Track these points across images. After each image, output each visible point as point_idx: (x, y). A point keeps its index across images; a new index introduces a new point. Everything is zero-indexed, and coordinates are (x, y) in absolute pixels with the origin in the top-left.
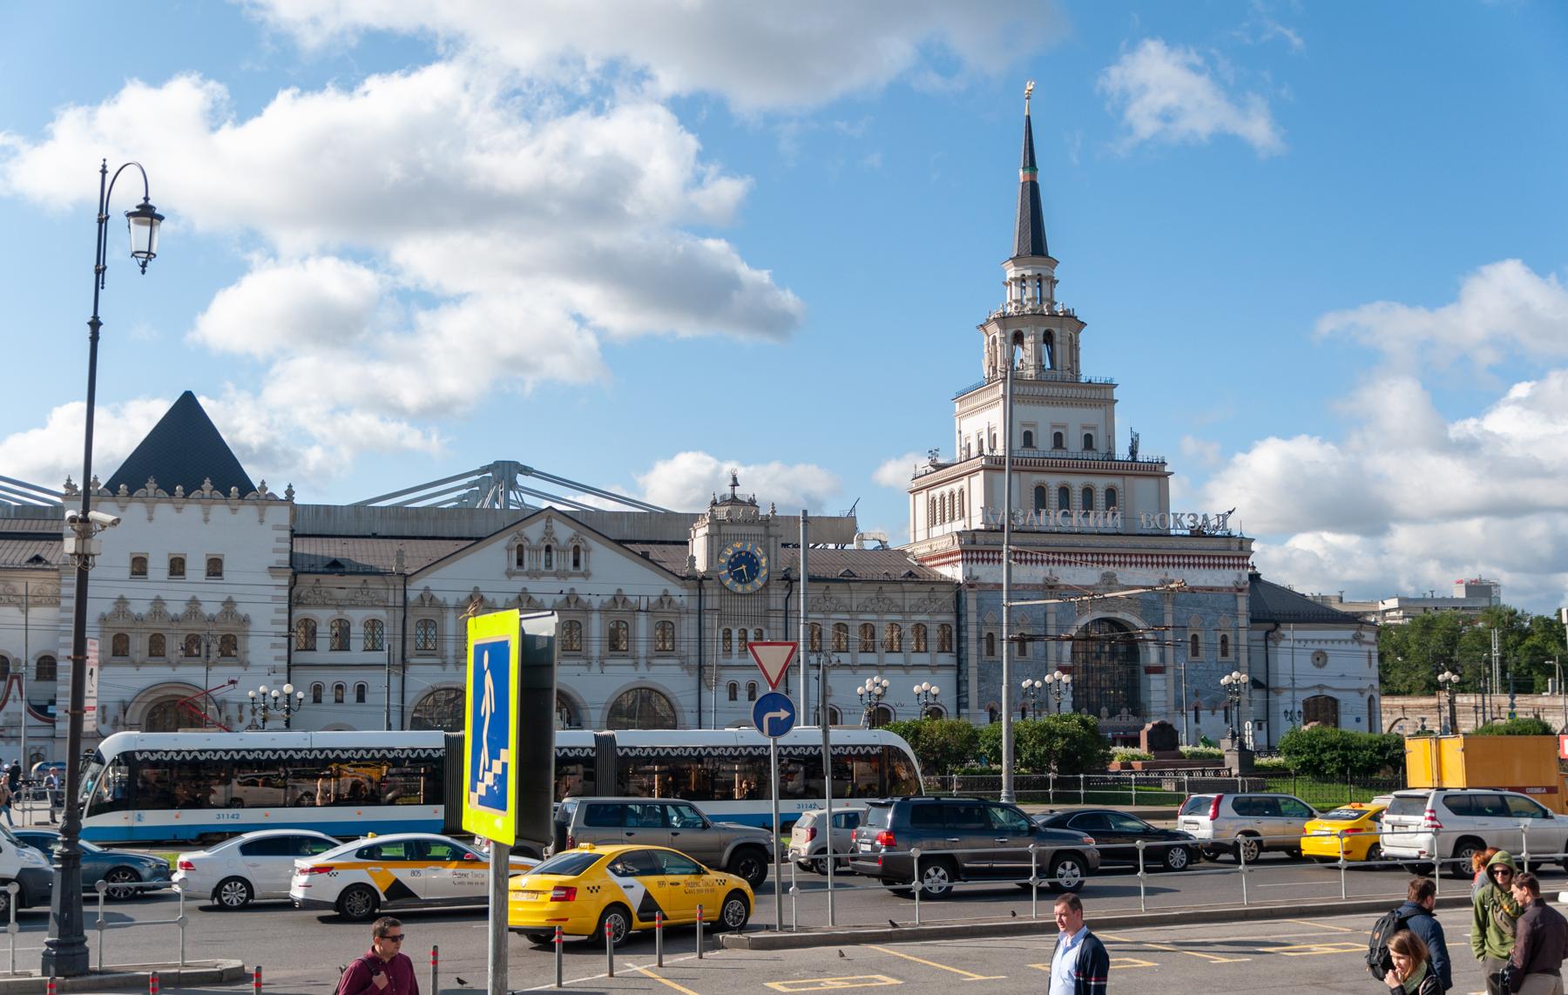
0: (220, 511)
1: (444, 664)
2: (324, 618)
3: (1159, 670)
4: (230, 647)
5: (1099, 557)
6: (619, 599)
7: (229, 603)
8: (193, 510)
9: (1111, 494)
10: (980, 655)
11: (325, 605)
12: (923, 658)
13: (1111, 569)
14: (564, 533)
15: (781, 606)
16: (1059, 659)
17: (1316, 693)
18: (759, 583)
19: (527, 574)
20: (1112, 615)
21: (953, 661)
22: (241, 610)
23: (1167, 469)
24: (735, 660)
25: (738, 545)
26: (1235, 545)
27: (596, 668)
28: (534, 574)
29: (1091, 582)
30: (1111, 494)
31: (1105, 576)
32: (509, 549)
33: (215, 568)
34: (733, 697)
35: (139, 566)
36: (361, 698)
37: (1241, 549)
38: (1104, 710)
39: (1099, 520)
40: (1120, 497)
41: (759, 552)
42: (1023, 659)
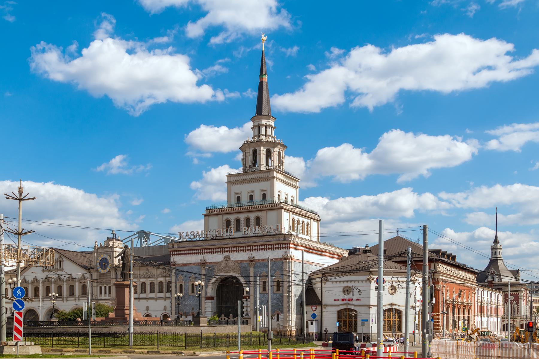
9: (258, 220)
12: (152, 295)
18: (108, 269)
20: (228, 274)
27: (65, 301)
29: (219, 261)
30: (258, 220)
37: (285, 239)
39: (253, 230)
40: (263, 221)
41: (108, 258)
42: (193, 294)
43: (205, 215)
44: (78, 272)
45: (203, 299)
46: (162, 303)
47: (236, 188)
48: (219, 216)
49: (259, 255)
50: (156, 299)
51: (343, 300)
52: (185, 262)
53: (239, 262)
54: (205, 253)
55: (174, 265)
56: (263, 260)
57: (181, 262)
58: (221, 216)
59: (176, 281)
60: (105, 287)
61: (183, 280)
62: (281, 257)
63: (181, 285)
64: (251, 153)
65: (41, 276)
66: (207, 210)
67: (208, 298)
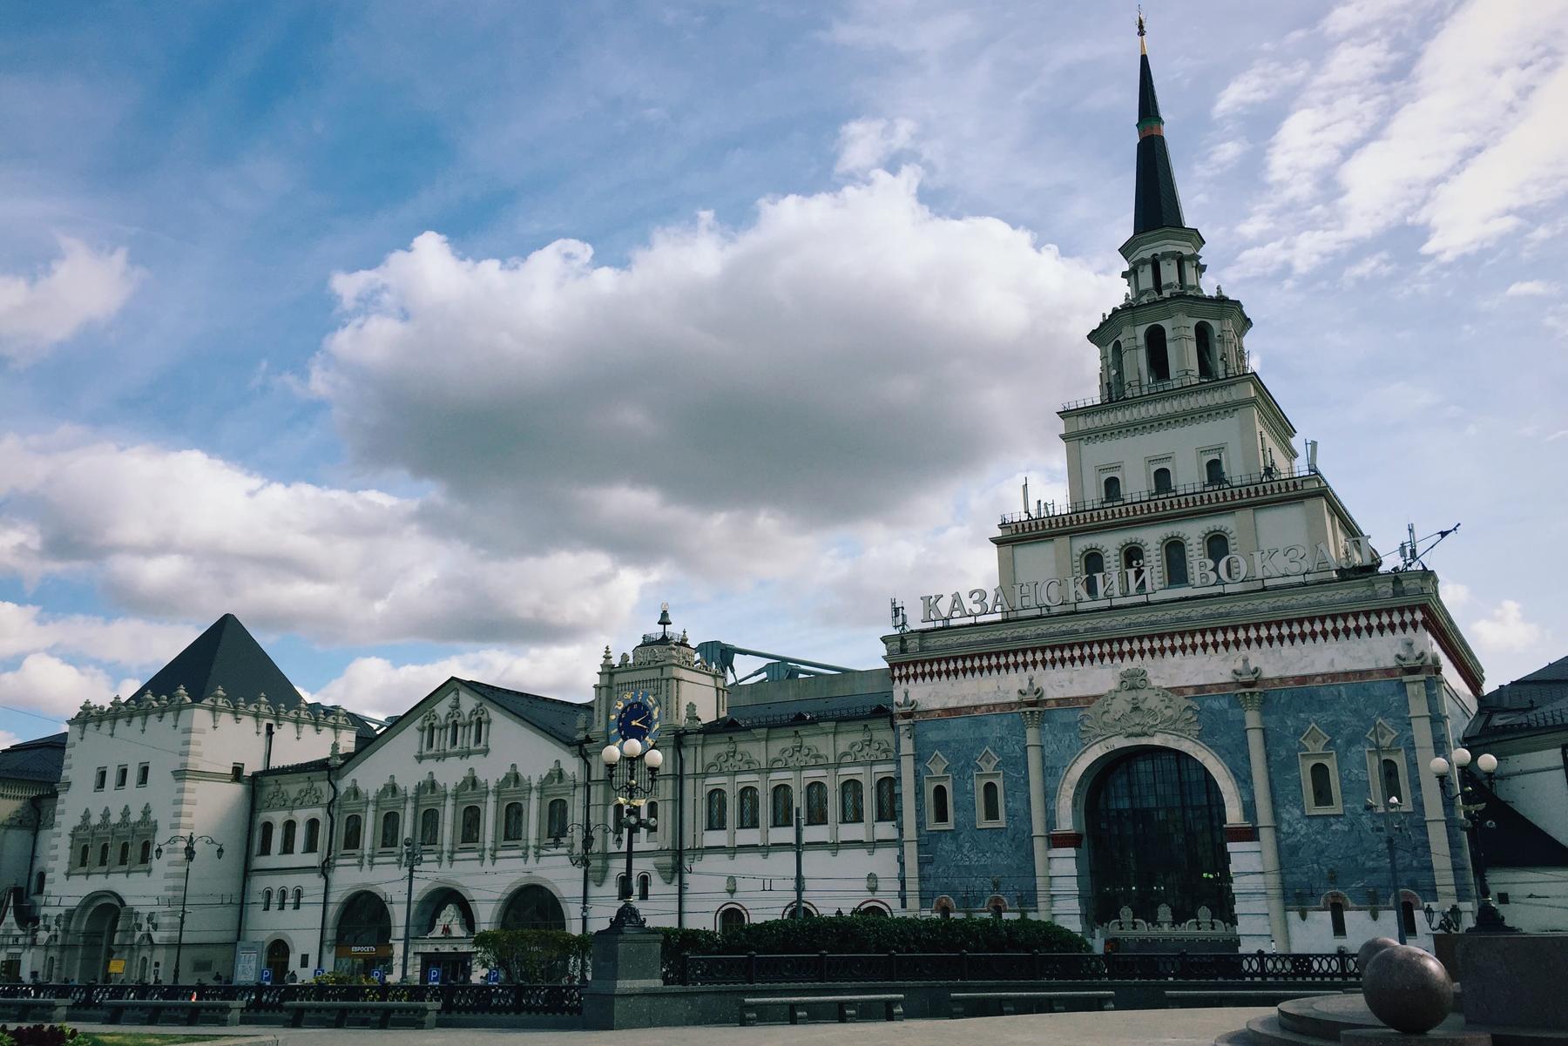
2: (278, 818)
3: (1248, 834)
5: (1109, 645)
10: (920, 825)
16: (1050, 821)
20: (1144, 741)
21: (895, 835)
30: (1217, 545)
31: (1125, 677)
32: (422, 730)
43: (998, 542)
45: (1039, 845)
46: (857, 864)
47: (1101, 453)
48: (1057, 540)
49: (1279, 662)
50: (835, 847)
52: (952, 704)
53: (1190, 693)
56: (1303, 679)
57: (935, 704)
58: (1067, 538)
59: (917, 775)
61: (946, 770)
62: (1390, 663)
63: (940, 792)
64: (1141, 341)
65: (409, 779)
66: (1003, 526)
67: (1057, 841)
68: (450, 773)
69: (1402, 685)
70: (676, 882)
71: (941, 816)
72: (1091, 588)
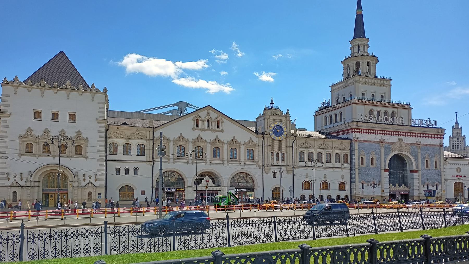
0: (74, 94)
1: (169, 162)
4: (79, 151)
5: (397, 133)
6: (234, 140)
7: (79, 132)
8: (62, 93)
10: (359, 165)
11: (121, 138)
13: (401, 137)
14: (214, 116)
15: (291, 145)
16: (385, 167)
17: (458, 181)
18: (283, 136)
19: (200, 130)
21: (349, 166)
22: (84, 136)
23: (411, 107)
24: (275, 164)
25: (276, 123)
26: (440, 131)
28: (203, 130)
30: (393, 114)
31: (399, 139)
32: (193, 120)
33: (72, 118)
34: (274, 176)
35: (37, 115)
36: (136, 174)
37: (442, 132)
38: (397, 185)
41: (283, 126)
42: (372, 166)
44: (243, 136)
51: (457, 176)
52: (365, 140)
54: (383, 134)
55: (356, 141)
56: (426, 145)
60: (278, 154)
63: (362, 158)
67: (386, 171)
68: (208, 136)
69: (440, 148)
70: (291, 175)
71: (362, 164)
72: (394, 120)
